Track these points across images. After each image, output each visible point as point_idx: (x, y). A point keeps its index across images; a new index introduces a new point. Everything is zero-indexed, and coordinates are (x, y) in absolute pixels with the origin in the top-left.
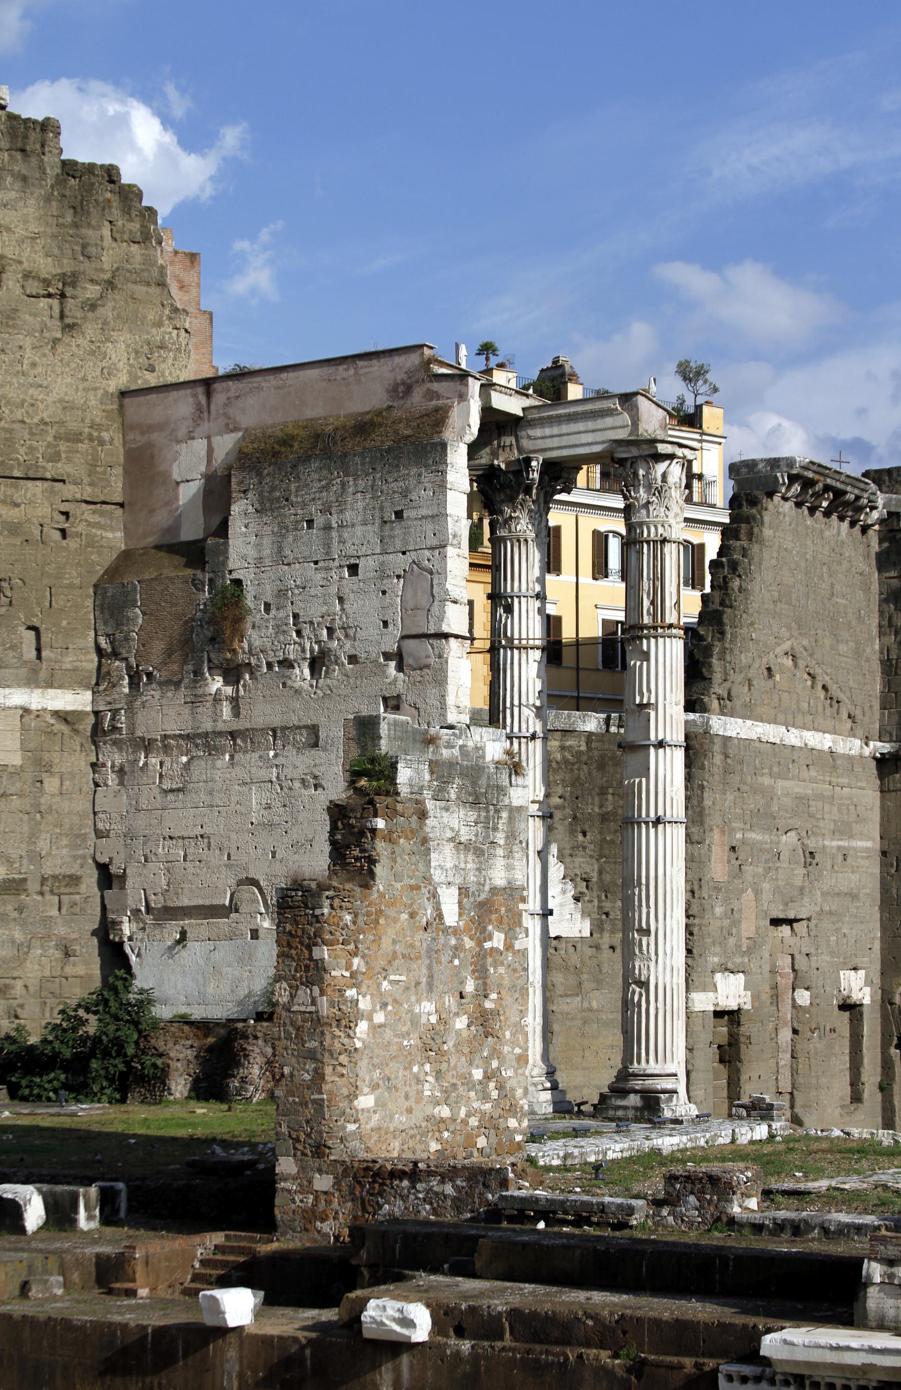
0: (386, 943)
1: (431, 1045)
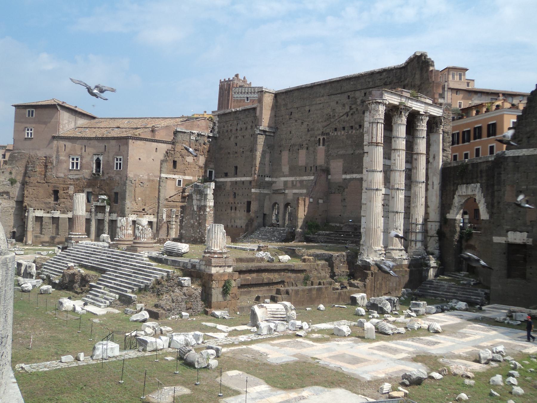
1: (192, 226)
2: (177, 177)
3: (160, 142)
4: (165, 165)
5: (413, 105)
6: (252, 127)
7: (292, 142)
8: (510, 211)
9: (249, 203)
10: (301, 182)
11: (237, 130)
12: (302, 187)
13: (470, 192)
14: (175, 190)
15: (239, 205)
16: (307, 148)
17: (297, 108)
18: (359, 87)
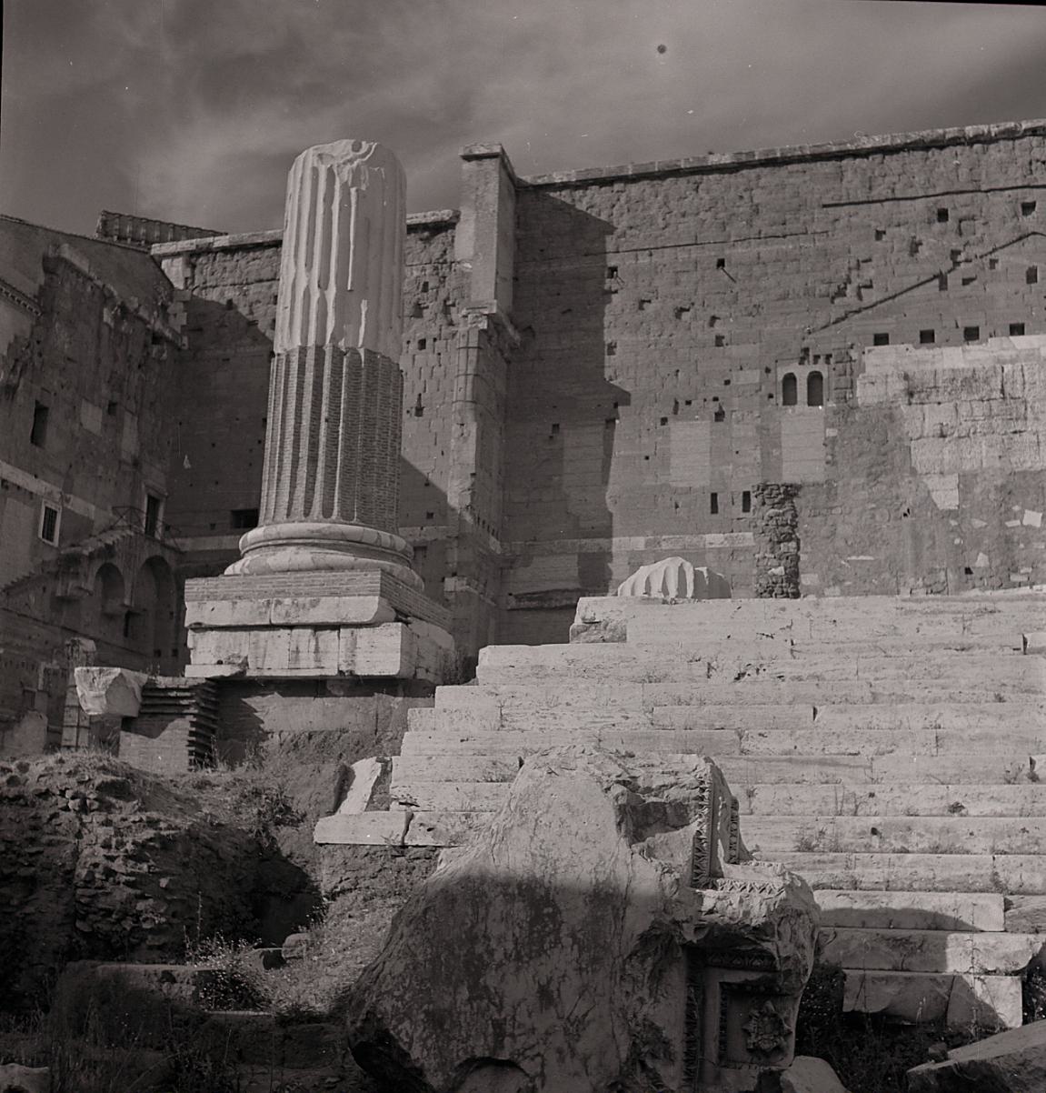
16: (719, 416)
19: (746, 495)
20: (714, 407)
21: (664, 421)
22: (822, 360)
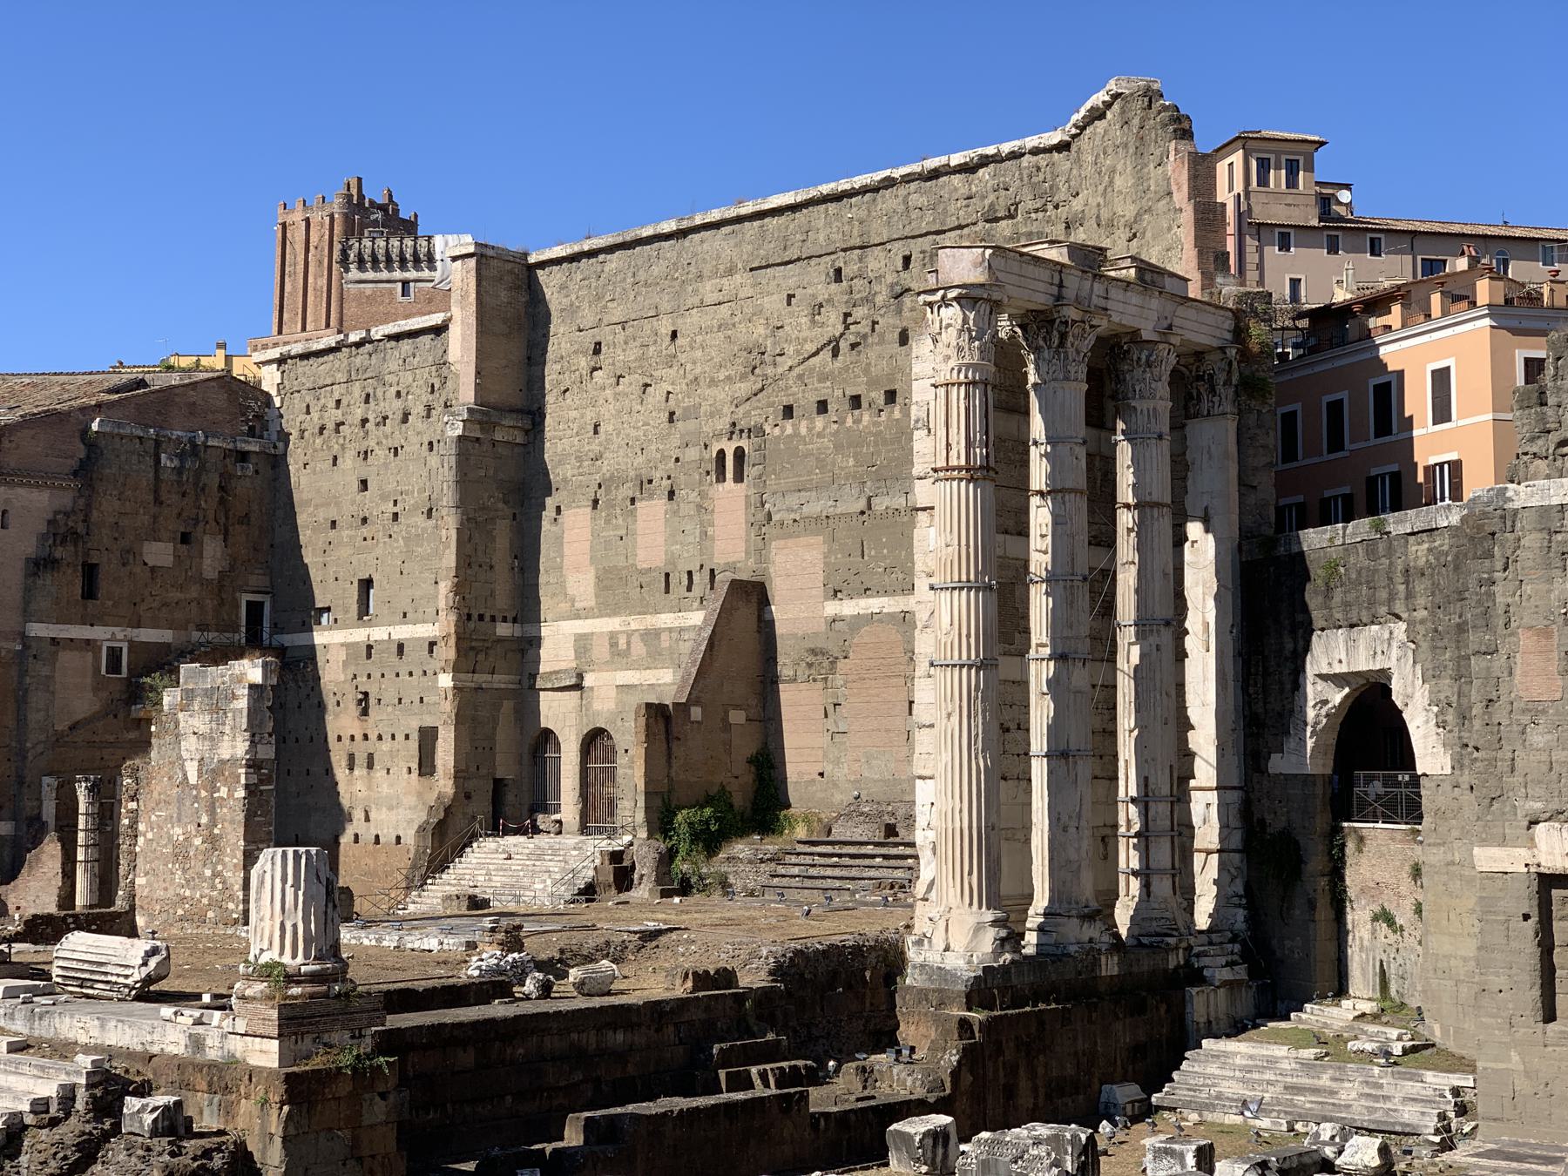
0: (155, 795)
1: (181, 854)
2: (98, 633)
3: (21, 485)
4: (47, 580)
5: (1110, 305)
6: (429, 409)
7: (606, 467)
8: (1538, 738)
9: (428, 737)
10: (651, 636)
11: (365, 421)
12: (654, 658)
13: (1363, 664)
14: (95, 690)
15: (386, 746)
16: (671, 494)
17: (623, 324)
18: (879, 232)
19: (690, 573)
20: (666, 483)
21: (633, 500)
22: (745, 435)
